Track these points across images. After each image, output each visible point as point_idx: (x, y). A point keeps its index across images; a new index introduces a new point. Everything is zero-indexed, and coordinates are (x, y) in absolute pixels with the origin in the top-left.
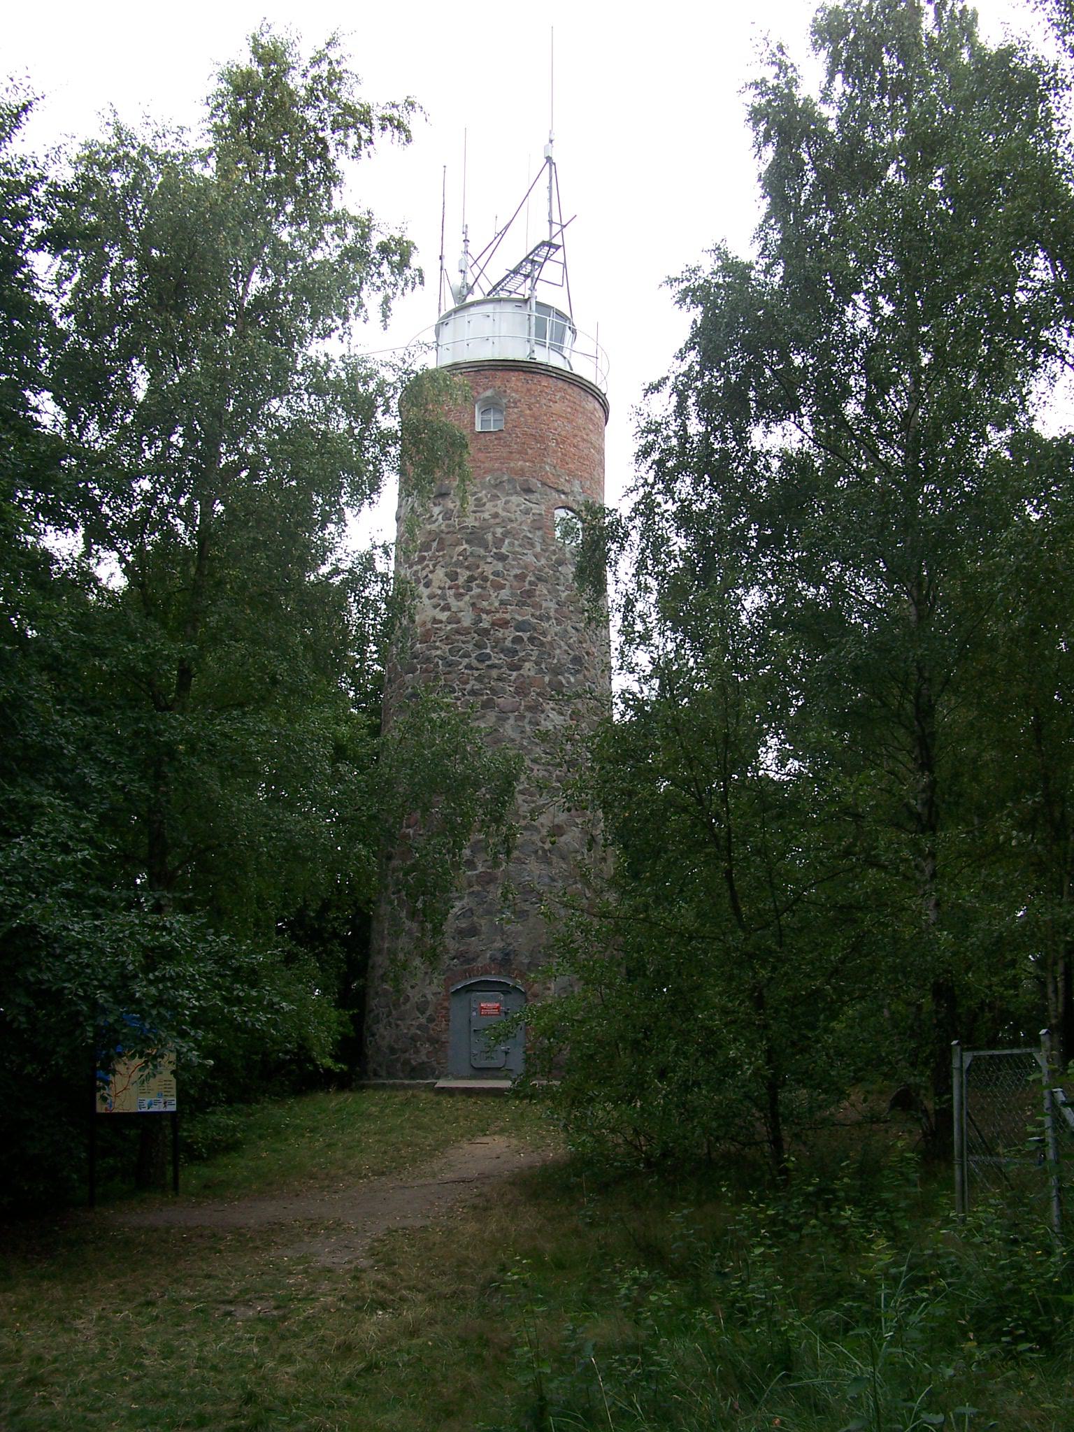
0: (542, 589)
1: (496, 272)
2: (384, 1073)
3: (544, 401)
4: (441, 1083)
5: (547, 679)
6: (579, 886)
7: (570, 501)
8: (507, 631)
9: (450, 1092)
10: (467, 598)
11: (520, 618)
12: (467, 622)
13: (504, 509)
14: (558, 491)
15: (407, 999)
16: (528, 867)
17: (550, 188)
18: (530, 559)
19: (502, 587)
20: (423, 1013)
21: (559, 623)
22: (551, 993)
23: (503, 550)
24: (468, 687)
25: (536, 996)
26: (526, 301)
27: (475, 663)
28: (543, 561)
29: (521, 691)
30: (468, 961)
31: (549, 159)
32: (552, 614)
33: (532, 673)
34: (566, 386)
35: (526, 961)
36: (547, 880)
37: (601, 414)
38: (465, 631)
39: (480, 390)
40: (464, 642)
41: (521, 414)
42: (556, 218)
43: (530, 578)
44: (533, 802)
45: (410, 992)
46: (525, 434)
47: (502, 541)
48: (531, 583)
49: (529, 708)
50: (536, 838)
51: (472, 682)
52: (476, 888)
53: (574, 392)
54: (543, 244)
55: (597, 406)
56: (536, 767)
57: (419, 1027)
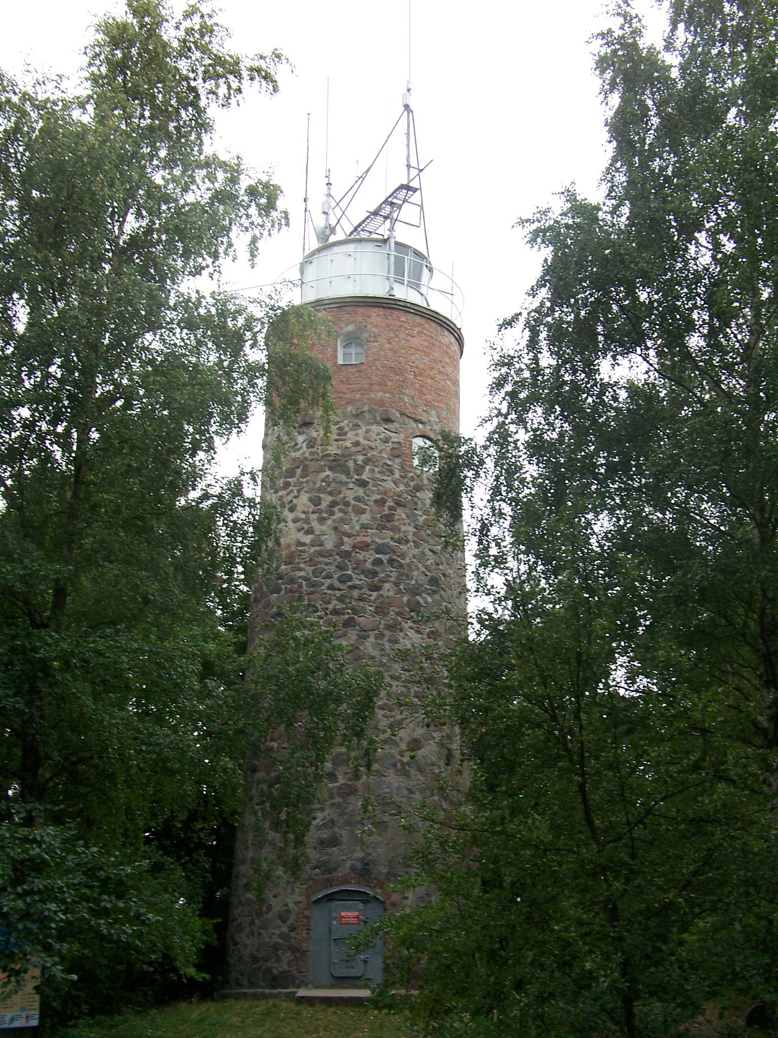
0: (401, 513)
1: (357, 214)
2: (245, 982)
3: (402, 336)
4: (302, 992)
5: (405, 599)
6: (436, 798)
7: (427, 430)
8: (367, 554)
9: (310, 1001)
10: (329, 522)
11: (380, 541)
12: (329, 545)
13: (366, 438)
14: (416, 420)
15: (270, 908)
16: (387, 780)
17: (408, 134)
18: (390, 485)
19: (363, 512)
20: (284, 921)
21: (417, 546)
22: (408, 902)
23: (364, 477)
24: (331, 606)
25: (394, 905)
26: (385, 241)
27: (337, 584)
28: (402, 487)
29: (381, 610)
30: (329, 871)
31: (407, 107)
32: (410, 537)
33: (391, 594)
34: (423, 322)
35: (385, 871)
36: (405, 792)
37: (456, 347)
38: (329, 554)
39: (342, 325)
40: (327, 564)
42: (413, 163)
43: (390, 503)
44: (392, 717)
45: (273, 901)
46: (384, 366)
47: (363, 468)
48: (390, 508)
49: (389, 627)
50: (395, 751)
51: (335, 602)
52: (338, 800)
53: (432, 327)
54: (402, 187)
55: (453, 340)
56: (395, 683)
57: (282, 936)
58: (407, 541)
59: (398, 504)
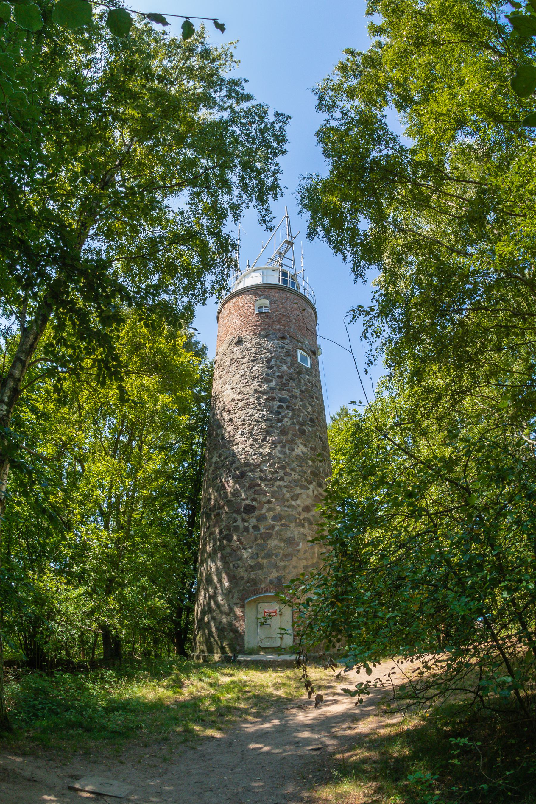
5: (297, 427)
8: (275, 403)
18: (285, 368)
19: (271, 381)
21: (302, 400)
28: (292, 370)
33: (289, 424)
41: (278, 306)
52: (260, 541)
56: (293, 473)
58: (296, 397)
59: (291, 378)
